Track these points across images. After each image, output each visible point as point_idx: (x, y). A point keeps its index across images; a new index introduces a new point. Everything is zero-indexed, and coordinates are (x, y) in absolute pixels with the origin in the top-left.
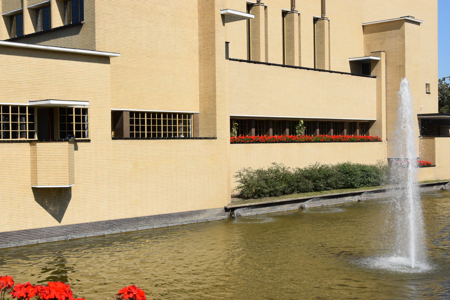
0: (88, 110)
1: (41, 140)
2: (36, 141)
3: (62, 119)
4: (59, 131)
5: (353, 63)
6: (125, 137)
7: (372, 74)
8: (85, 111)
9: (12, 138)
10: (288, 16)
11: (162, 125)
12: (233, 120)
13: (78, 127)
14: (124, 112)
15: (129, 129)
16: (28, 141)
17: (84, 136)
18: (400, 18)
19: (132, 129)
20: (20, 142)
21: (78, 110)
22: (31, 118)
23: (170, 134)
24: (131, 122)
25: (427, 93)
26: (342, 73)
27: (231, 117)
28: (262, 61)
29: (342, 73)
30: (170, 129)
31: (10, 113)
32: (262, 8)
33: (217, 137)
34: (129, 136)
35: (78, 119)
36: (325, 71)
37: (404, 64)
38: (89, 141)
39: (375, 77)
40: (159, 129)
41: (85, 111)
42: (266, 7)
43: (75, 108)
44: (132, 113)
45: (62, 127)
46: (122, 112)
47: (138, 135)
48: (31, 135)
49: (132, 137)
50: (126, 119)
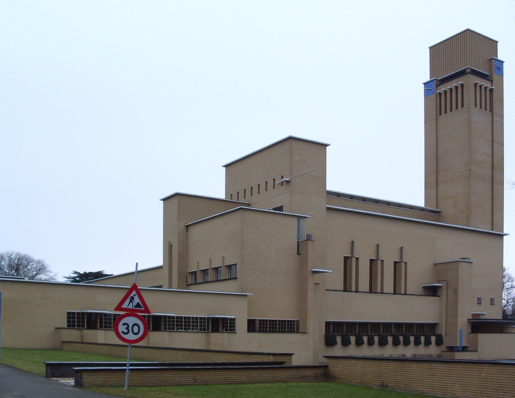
1: (213, 331)
2: (210, 332)
3: (223, 323)
5: (425, 288)
7: (438, 294)
12: (328, 324)
13: (230, 326)
14: (256, 320)
19: (260, 327)
21: (231, 319)
22: (208, 323)
24: (260, 324)
25: (491, 304)
26: (412, 295)
27: (325, 321)
29: (412, 295)
30: (282, 328)
35: (230, 323)
36: (401, 294)
38: (236, 333)
39: (439, 296)
41: (234, 319)
44: (260, 320)
45: (223, 326)
46: (255, 320)
48: (208, 330)
49: (260, 331)
50: (257, 323)
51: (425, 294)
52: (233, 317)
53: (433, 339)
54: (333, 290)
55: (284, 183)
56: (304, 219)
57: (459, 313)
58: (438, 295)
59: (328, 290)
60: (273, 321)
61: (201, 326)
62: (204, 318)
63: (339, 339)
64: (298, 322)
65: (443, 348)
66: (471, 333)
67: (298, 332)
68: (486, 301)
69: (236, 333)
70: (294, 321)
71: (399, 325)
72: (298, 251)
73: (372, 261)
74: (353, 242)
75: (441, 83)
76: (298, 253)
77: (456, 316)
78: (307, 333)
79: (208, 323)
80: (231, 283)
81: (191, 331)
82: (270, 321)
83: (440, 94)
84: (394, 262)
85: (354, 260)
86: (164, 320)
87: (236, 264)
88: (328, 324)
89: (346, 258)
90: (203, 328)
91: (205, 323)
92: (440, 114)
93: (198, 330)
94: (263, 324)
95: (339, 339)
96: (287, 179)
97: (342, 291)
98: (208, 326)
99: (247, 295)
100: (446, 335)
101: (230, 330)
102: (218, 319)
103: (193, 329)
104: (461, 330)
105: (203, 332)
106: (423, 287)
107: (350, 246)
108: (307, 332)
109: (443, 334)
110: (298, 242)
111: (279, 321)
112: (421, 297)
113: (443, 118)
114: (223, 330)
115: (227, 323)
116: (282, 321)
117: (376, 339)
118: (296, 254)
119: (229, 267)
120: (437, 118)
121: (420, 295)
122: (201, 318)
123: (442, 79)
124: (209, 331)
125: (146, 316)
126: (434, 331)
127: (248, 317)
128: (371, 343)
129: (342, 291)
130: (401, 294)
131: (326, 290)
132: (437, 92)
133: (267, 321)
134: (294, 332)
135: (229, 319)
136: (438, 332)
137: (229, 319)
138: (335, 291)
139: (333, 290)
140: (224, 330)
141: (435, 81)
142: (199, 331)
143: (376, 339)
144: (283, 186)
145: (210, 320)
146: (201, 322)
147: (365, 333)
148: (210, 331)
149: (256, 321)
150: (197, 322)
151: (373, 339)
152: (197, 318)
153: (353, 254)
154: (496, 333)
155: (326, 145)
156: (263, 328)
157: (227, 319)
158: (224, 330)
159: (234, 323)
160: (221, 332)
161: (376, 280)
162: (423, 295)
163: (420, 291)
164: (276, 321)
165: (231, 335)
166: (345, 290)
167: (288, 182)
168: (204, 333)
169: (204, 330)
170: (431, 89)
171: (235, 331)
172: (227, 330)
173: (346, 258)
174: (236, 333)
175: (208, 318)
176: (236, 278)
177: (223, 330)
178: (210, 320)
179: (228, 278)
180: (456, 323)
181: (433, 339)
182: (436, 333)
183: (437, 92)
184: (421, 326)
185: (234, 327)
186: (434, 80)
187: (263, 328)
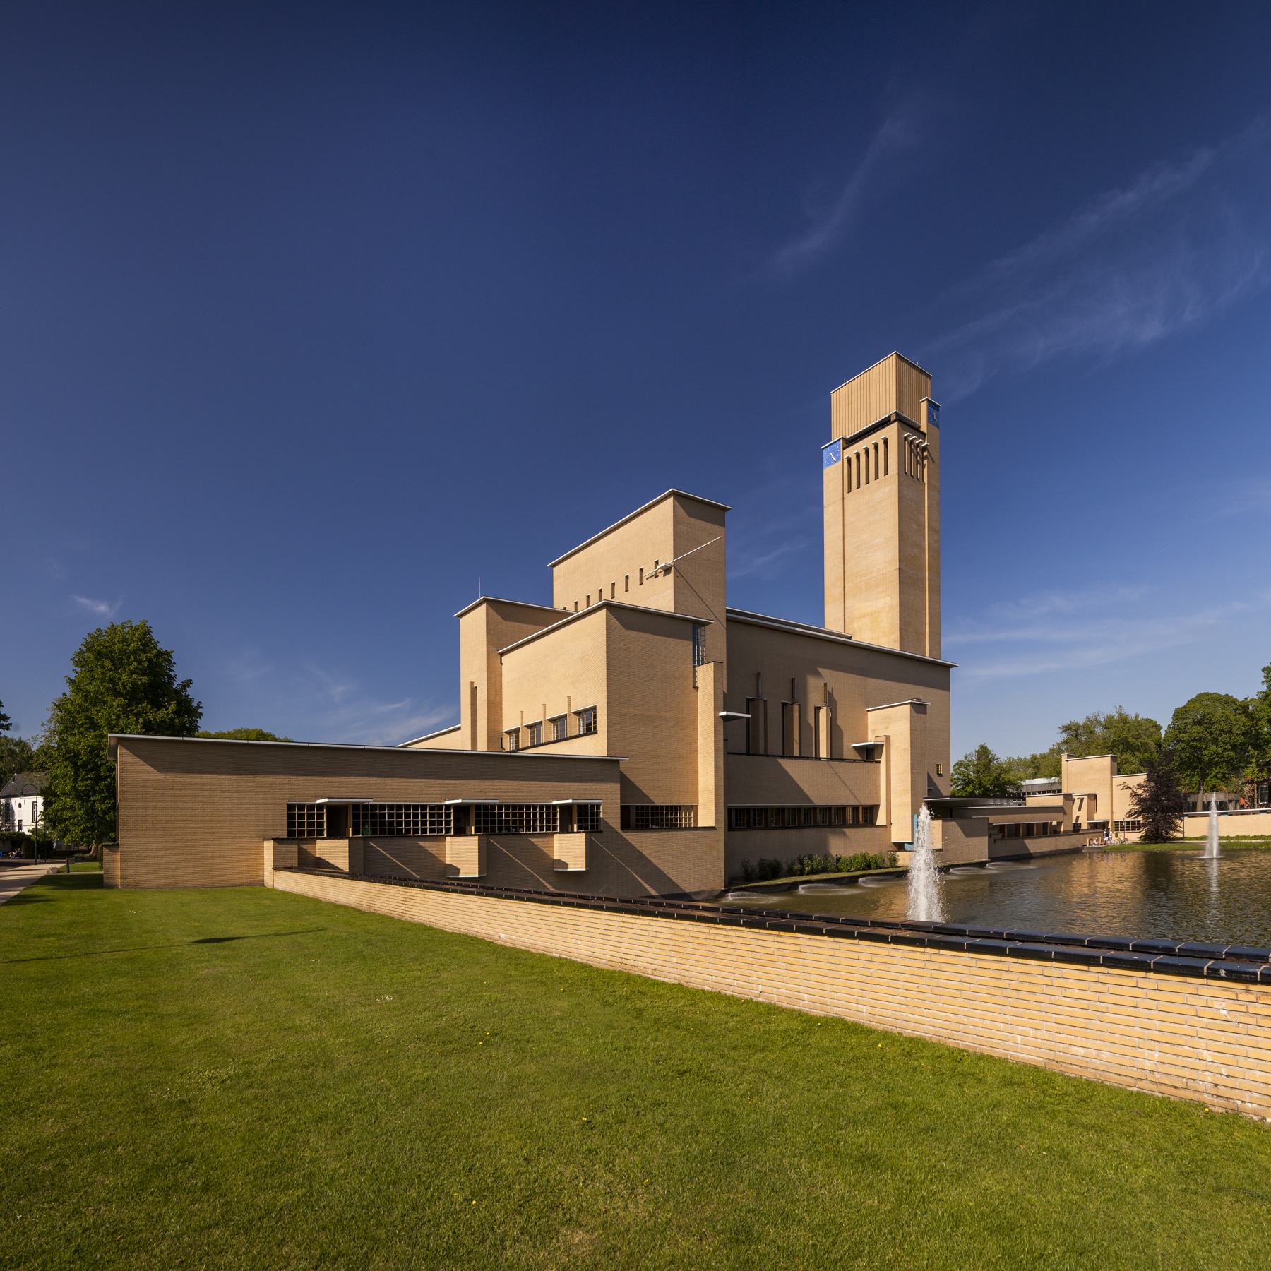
3: (579, 814)
8: (598, 806)
13: (592, 820)
15: (635, 820)
17: (597, 829)
19: (638, 820)
21: (592, 806)
24: (637, 814)
44: (637, 807)
47: (643, 826)
50: (633, 812)
56: (703, 628)
59: (733, 753)
86: (476, 814)
98: (555, 821)
99: (619, 760)
124: (556, 830)
125: (861, 811)
130: (843, 760)
138: (739, 754)
149: (631, 809)
166: (748, 754)
174: (601, 832)
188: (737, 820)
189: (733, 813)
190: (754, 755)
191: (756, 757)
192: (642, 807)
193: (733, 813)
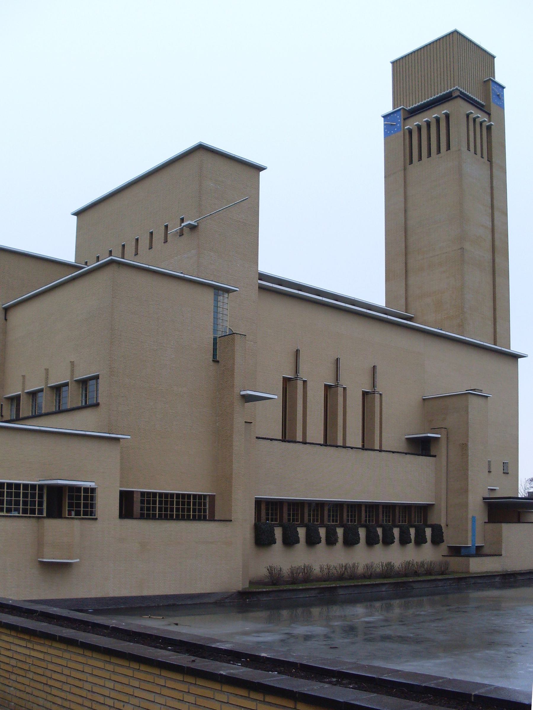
0: (97, 489)
1: (50, 516)
2: (45, 517)
3: (71, 498)
4: (67, 509)
5: (411, 441)
6: (134, 517)
9: (22, 514)
10: (333, 389)
11: (175, 506)
12: (258, 502)
13: (86, 505)
16: (36, 517)
18: (466, 391)
19: (142, 509)
20: (30, 517)
21: (86, 490)
22: (41, 496)
23: (183, 516)
24: (142, 502)
26: (393, 452)
28: (298, 440)
29: (393, 452)
30: (183, 510)
31: (21, 491)
32: (300, 384)
33: (232, 519)
34: (139, 516)
35: (86, 498)
37: (468, 441)
38: (96, 519)
39: (435, 456)
40: (172, 510)
41: (93, 490)
42: (305, 382)
43: (83, 488)
44: (143, 494)
45: (70, 505)
48: (41, 512)
49: (142, 517)
50: (137, 499)
51: (410, 452)
52: (92, 485)
53: (428, 532)
54: (268, 439)
55: (186, 230)
57: (470, 487)
58: (432, 454)
60: (166, 495)
61: (25, 503)
62: (33, 487)
63: (278, 533)
64: (212, 497)
65: (443, 548)
66: (487, 522)
67: (212, 519)
68: (497, 469)
69: (97, 521)
70: (205, 496)
71: (372, 507)
72: (215, 355)
73: (327, 387)
74: (297, 351)
75: (409, 116)
76: (215, 361)
77: (465, 491)
78: (231, 521)
79: (41, 496)
80: (87, 414)
81: (5, 514)
82: (161, 495)
83: (410, 132)
84: (363, 391)
85: (300, 384)
87: (97, 378)
88: (258, 502)
89: (286, 380)
90: (30, 506)
91: (33, 495)
92: (411, 162)
93: (19, 513)
94: (148, 503)
95: (278, 533)
96: (192, 223)
97: (279, 440)
98: (41, 504)
100: (447, 525)
101: (85, 513)
102: (60, 488)
103: (9, 510)
104: (473, 518)
105: (30, 517)
106: (407, 439)
107: (292, 359)
108: (233, 518)
109: (443, 525)
110: (215, 339)
111: (178, 495)
112: (408, 456)
113: (416, 169)
114: (70, 514)
115: (79, 498)
116: (183, 495)
117: (340, 532)
118: (212, 362)
119: (84, 383)
120: (405, 169)
121: (406, 454)
122: (26, 486)
123: (412, 108)
126: (425, 520)
127: (121, 487)
128: (331, 541)
129: (279, 440)
131: (257, 438)
132: (406, 128)
133: (154, 494)
134: (205, 519)
135: (82, 488)
136: (433, 519)
137: (82, 488)
139: (268, 439)
140: (73, 513)
141: (402, 111)
142: (21, 515)
143: (340, 532)
144: (183, 236)
145: (45, 491)
146: (25, 495)
147: (336, 522)
148: (45, 515)
150: (17, 495)
151: (335, 533)
152: (18, 486)
153: (299, 373)
154: (507, 523)
155: (260, 169)
156: (148, 509)
157: (78, 489)
158: (73, 513)
159: (92, 498)
160: (66, 518)
161: (335, 424)
162: (409, 454)
163: (402, 446)
164: (172, 495)
165: (88, 524)
167: (193, 228)
168: (32, 519)
169: (33, 511)
170: (395, 124)
171: (95, 516)
172: (78, 513)
173: (286, 380)
174: (96, 519)
175: (41, 487)
176: (97, 405)
177: (70, 514)
178: (45, 491)
179: (80, 405)
180: (465, 505)
181: (428, 532)
182: (429, 522)
183: (406, 128)
184: (407, 508)
185: (92, 506)
186: (400, 110)
187: (148, 509)
188: (267, 514)
189: (263, 507)
190: (289, 442)
191: (291, 445)
192: (149, 493)
193: (263, 507)
